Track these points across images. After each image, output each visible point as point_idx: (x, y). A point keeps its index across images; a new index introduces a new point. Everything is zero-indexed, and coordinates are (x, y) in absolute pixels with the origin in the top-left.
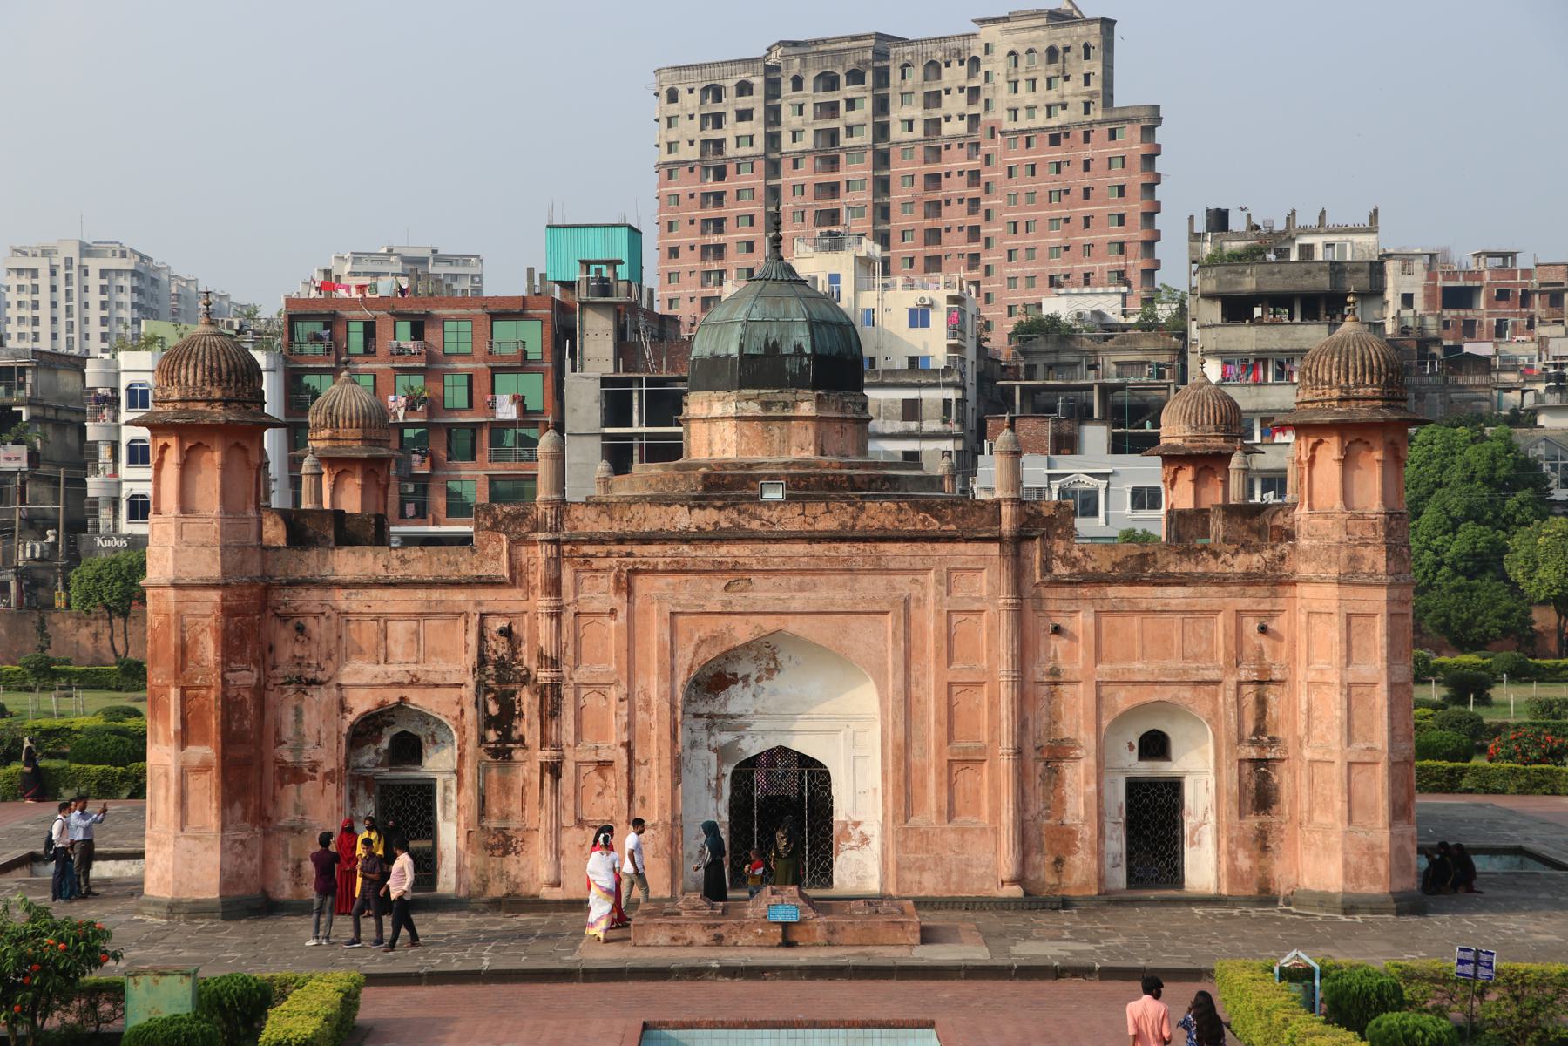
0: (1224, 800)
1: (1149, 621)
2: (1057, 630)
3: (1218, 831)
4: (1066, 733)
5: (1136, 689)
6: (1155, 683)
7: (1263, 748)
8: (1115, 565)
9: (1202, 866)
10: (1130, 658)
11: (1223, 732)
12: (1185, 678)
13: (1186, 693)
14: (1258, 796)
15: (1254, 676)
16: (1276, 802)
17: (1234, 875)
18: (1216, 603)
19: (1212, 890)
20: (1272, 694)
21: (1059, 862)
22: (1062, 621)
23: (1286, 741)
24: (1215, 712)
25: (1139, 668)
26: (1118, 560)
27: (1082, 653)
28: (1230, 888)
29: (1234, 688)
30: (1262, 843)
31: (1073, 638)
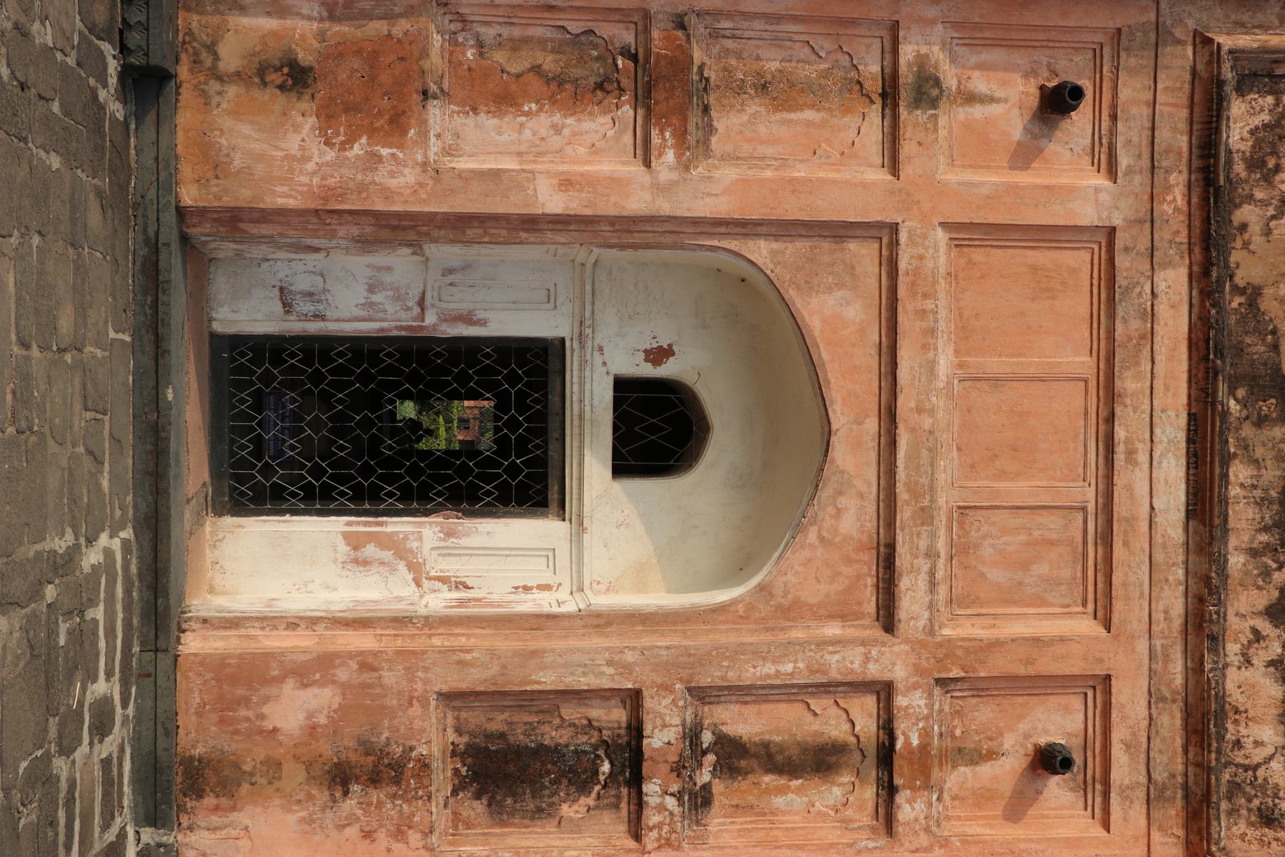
0: (506, 643)
1: (1071, 406)
2: (1058, 102)
3: (401, 621)
4: (732, 122)
5: (868, 358)
6: (889, 415)
7: (678, 769)
8: (1253, 294)
9: (281, 574)
10: (965, 335)
11: (727, 637)
12: (905, 514)
13: (850, 513)
14: (518, 752)
15: (908, 736)
16: (498, 813)
17: (248, 677)
18: (1131, 612)
19: (200, 603)
20: (846, 794)
21: (297, 77)
22: (1080, 122)
23: (699, 842)
24: (791, 611)
25: (932, 367)
26: (1268, 304)
27: (981, 185)
28: (203, 661)
29: (874, 671)
30: (362, 770)
31: (1024, 156)
